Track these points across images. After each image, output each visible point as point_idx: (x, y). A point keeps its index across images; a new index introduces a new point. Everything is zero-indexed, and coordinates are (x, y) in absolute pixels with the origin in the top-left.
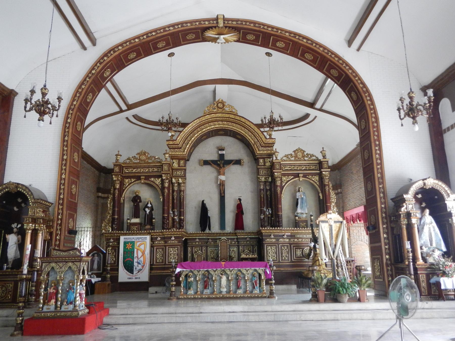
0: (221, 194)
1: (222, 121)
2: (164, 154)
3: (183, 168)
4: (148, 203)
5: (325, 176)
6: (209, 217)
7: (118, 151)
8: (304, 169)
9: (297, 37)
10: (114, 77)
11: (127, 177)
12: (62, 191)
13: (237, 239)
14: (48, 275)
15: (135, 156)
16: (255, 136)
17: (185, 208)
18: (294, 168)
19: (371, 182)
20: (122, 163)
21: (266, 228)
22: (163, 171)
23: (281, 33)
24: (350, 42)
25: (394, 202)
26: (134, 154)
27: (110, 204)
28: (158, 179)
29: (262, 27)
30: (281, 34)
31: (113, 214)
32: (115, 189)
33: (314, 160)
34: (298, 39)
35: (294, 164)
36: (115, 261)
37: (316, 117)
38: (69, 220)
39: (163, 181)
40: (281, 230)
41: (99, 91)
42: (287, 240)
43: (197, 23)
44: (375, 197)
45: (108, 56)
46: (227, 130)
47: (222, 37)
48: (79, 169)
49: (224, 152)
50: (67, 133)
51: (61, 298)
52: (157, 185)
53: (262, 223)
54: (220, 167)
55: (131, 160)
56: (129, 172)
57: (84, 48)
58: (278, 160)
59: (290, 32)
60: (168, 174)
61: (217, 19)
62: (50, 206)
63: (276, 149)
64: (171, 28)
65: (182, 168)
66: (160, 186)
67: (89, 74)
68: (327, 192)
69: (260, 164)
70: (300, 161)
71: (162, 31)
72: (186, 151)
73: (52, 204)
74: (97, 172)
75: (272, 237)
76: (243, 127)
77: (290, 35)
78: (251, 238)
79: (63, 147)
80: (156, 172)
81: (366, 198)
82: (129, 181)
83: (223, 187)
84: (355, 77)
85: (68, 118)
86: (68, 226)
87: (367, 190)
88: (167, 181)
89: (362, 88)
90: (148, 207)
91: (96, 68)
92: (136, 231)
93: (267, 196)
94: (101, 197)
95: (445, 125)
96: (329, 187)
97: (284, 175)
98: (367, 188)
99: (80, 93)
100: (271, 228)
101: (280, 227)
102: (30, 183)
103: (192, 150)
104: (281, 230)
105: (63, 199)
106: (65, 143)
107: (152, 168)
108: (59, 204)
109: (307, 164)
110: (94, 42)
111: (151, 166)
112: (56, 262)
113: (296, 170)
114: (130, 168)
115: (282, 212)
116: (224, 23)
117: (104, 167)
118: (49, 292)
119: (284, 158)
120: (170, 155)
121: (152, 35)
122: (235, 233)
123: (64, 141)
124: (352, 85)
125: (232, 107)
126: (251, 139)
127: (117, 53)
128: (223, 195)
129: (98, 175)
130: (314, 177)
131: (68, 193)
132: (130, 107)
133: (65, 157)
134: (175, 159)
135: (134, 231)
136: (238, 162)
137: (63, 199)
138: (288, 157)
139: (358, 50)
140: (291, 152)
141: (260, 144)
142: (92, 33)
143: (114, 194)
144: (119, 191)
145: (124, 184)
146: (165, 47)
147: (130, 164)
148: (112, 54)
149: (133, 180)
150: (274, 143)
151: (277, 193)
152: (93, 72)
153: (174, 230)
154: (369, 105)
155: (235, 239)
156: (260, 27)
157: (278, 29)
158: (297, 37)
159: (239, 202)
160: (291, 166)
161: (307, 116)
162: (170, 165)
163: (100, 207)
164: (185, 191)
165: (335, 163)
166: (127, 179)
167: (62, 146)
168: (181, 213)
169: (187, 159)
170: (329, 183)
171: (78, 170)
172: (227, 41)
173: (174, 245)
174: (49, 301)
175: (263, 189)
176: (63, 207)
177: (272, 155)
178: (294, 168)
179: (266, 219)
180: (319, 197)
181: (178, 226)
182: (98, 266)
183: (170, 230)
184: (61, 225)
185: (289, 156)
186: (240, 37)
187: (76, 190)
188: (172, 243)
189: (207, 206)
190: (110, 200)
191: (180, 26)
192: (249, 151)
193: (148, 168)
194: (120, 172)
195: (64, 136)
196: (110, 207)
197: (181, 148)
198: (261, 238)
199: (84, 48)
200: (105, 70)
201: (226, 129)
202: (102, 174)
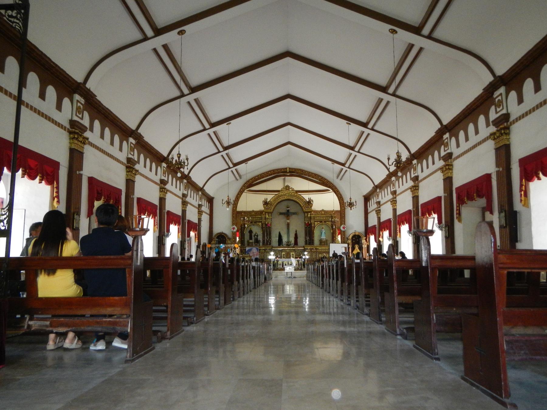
24: (338, 177)
34: (317, 177)
39: (262, 224)
42: (315, 250)
49: (289, 209)
57: (237, 180)
59: (314, 174)
61: (286, 168)
64: (270, 172)
78: (301, 249)
85: (234, 208)
90: (256, 235)
95: (369, 211)
97: (316, 221)
99: (237, 199)
102: (222, 231)
116: (289, 170)
123: (233, 216)
125: (293, 189)
127: (250, 183)
139: (341, 179)
152: (242, 190)
156: (302, 172)
157: (309, 172)
168: (270, 238)
175: (307, 227)
181: (268, 243)
195: (233, 215)
199: (237, 180)
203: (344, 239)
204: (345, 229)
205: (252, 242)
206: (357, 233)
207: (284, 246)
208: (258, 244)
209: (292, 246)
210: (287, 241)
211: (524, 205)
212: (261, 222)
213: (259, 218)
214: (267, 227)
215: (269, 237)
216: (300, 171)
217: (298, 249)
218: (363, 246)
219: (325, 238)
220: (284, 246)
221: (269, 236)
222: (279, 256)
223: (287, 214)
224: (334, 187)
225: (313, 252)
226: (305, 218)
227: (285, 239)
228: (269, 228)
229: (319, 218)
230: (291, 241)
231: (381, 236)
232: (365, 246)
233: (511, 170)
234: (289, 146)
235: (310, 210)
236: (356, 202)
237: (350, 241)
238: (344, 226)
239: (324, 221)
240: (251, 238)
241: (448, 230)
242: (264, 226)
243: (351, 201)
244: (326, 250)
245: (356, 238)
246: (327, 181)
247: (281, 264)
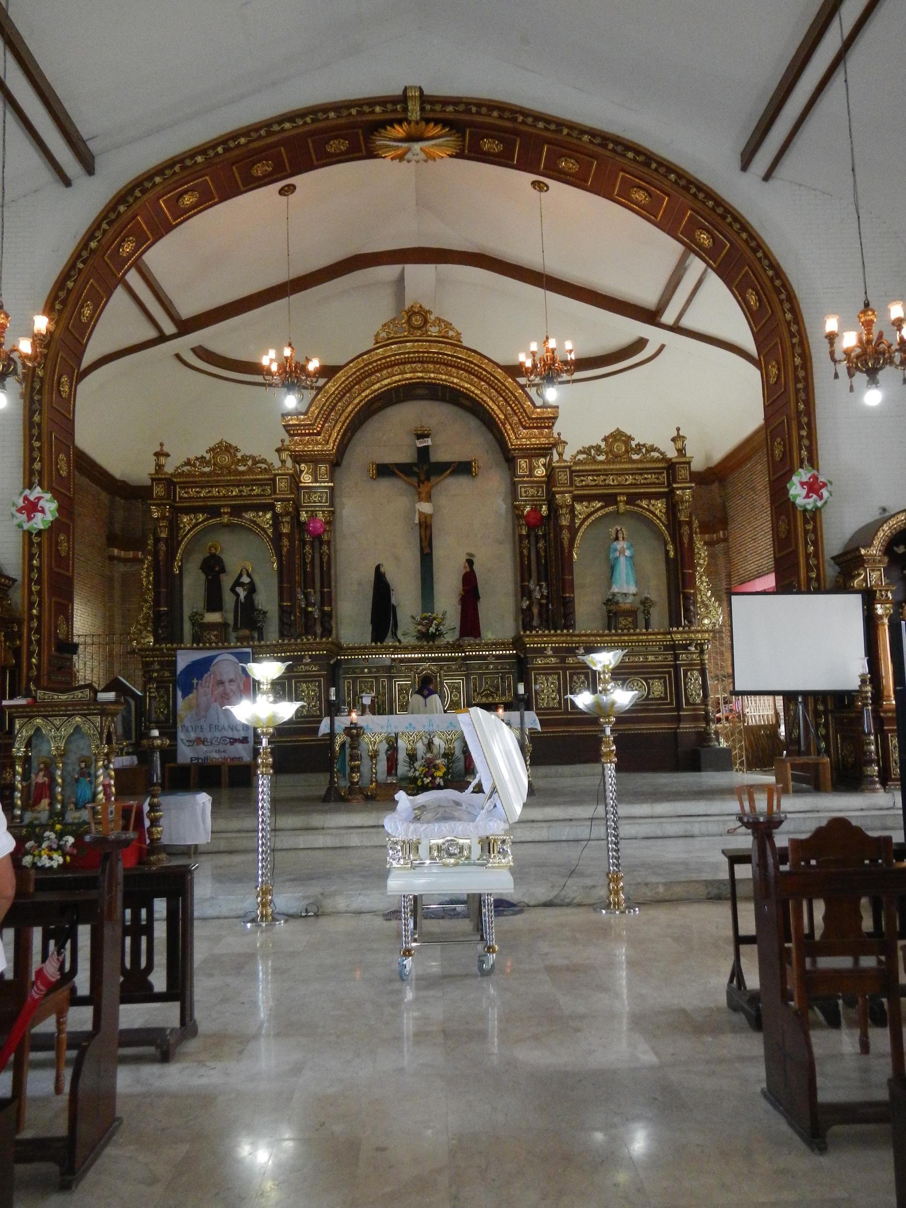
0: (422, 549)
1: (422, 362)
2: (278, 450)
3: (326, 484)
4: (240, 576)
5: (682, 502)
6: (394, 608)
7: (162, 445)
8: (631, 484)
9: (611, 146)
10: (144, 257)
11: (188, 511)
12: (35, 550)
14: (29, 744)
15: (205, 455)
16: (505, 400)
17: (333, 584)
18: (605, 480)
19: (788, 517)
20: (171, 475)
21: (534, 632)
22: (274, 492)
23: (568, 134)
24: (746, 160)
25: (838, 564)
26: (202, 452)
27: (148, 576)
28: (264, 515)
29: (520, 119)
30: (569, 139)
31: (157, 602)
32: (157, 540)
33: (657, 460)
34: (613, 150)
35: (605, 470)
36: (167, 716)
37: (662, 347)
38: (57, 617)
40: (572, 635)
41: (109, 295)
43: (354, 111)
44: (795, 552)
45: (128, 202)
46: (435, 384)
47: (417, 147)
48: (72, 496)
49: (428, 442)
50: (36, 406)
51: (63, 795)
52: (263, 529)
53: (525, 619)
54: (420, 482)
55: (194, 465)
56: (190, 498)
57: (67, 182)
58: (565, 461)
59: (593, 133)
60: (288, 500)
61: (403, 99)
62: (10, 587)
63: (559, 434)
64: (287, 125)
65: (323, 484)
66: (270, 531)
67: (82, 250)
68: (686, 540)
69: (520, 472)
70: (621, 462)
71: (263, 132)
72: (331, 441)
73: (14, 581)
74: (104, 497)
75: (550, 653)
76: (477, 376)
77: (591, 142)
78: (498, 657)
79: (31, 440)
80: (258, 495)
81: (774, 557)
82: (191, 520)
83: (428, 532)
84: (755, 251)
86: (56, 634)
87: (778, 536)
88: (288, 519)
89: (771, 280)
90: (242, 585)
91: (98, 234)
92: (217, 643)
93: (538, 552)
94: (119, 559)
96: (691, 528)
98: (777, 533)
99: (64, 302)
100: (547, 632)
101: (567, 628)
103: (347, 437)
104: (572, 635)
105: (39, 569)
106: (35, 431)
107: (247, 486)
108: (30, 580)
109: (638, 469)
110: (88, 163)
111: (246, 480)
112: (45, 717)
113: (609, 485)
114: (192, 487)
115: (573, 593)
116: (422, 109)
117: (124, 482)
118: (33, 783)
119: (581, 457)
120: (291, 451)
121: (239, 145)
122: (460, 646)
124: (747, 272)
125: (448, 325)
126: (496, 408)
128: (427, 551)
129: (107, 502)
130: (653, 502)
131: (50, 557)
132: (186, 327)
133: (37, 466)
134: (306, 462)
135: (210, 644)
136: (464, 468)
137: (39, 569)
138: (589, 454)
139: (767, 177)
140: (596, 439)
141: (520, 420)
142: (84, 142)
143: (156, 554)
144: (167, 546)
145: (179, 529)
146: (270, 174)
147: (194, 476)
148: (137, 198)
149: (201, 517)
150: (555, 418)
151: (562, 543)
152: (93, 245)
153: (308, 640)
154: (788, 323)
155: (459, 660)
156: (514, 120)
157: (560, 124)
158: (611, 146)
159: (468, 569)
160: (598, 476)
161: (641, 343)
162: (295, 478)
163: (117, 585)
164: (333, 543)
165: (712, 465)
166: (187, 514)
167: (27, 439)
169: (335, 461)
170: (690, 517)
171: (70, 498)
172: (430, 157)
173: (311, 676)
174: (37, 801)
176: (41, 589)
177: (550, 449)
178: (605, 480)
179: (535, 611)
180: (667, 552)
181: (319, 631)
182: (124, 728)
183: (299, 640)
184: (38, 631)
185: (593, 452)
186: (464, 146)
187: (69, 546)
188: (306, 671)
189: (389, 577)
190: (147, 568)
191: (308, 120)
192: (490, 436)
193: (238, 486)
194: (169, 498)
196: (148, 584)
197: (319, 434)
198: (522, 656)
199: (67, 182)
200: (123, 240)
201: (428, 383)
202: (117, 499)
203: (817, 567)
204: (825, 492)
205: (224, 625)
207: (405, 641)
208: (256, 635)
209: (450, 638)
210: (418, 618)
212: (271, 507)
214: (308, 538)
215: (322, 593)
216: (495, 114)
217: (485, 658)
219: (633, 589)
220: (405, 641)
221: (322, 587)
222: (367, 701)
224: (729, 220)
226: (514, 485)
228: (321, 543)
230: (444, 614)
235: (544, 441)
237: (874, 577)
238: (815, 478)
239: (627, 494)
240: (214, 602)
242: (285, 530)
244: (651, 658)
246: (683, 182)
247: (383, 757)
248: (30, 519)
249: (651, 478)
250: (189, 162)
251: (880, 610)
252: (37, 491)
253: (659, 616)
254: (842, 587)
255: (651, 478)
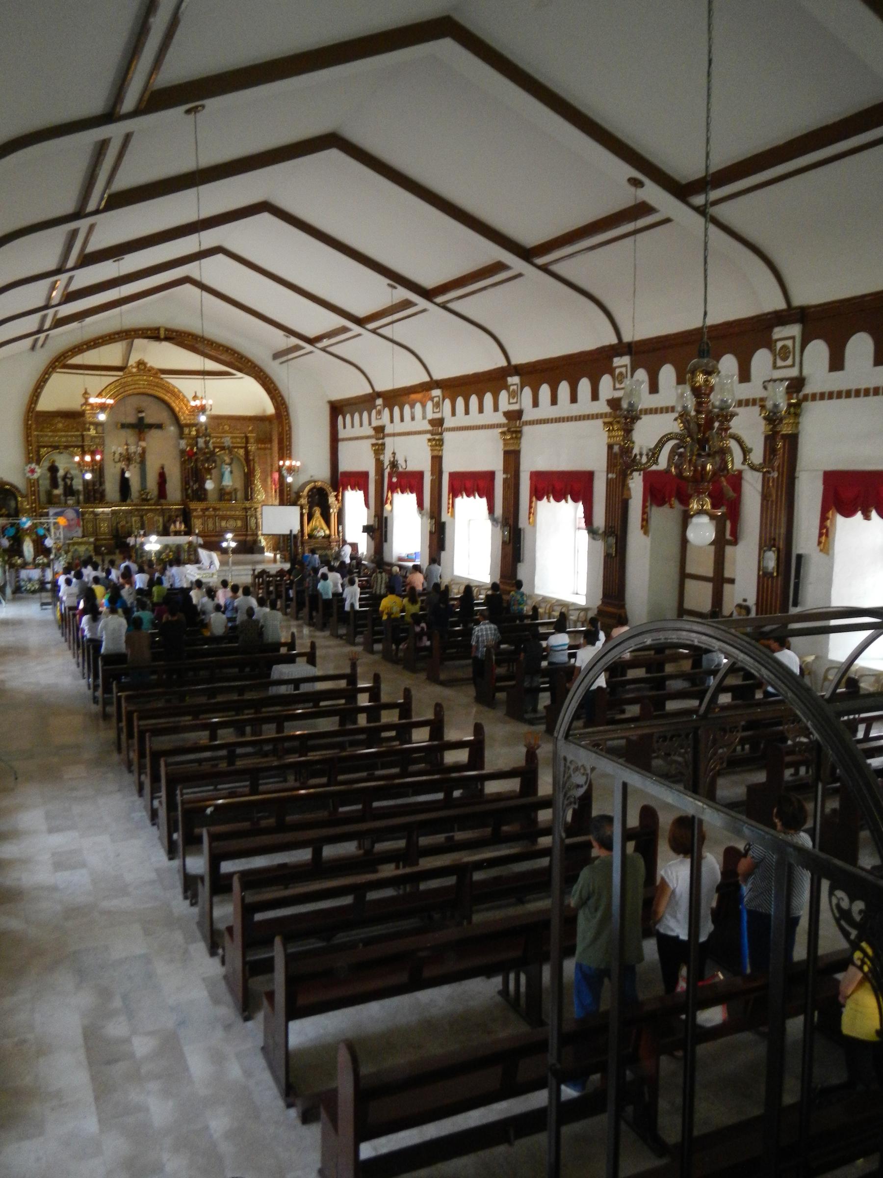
5: (250, 451)
11: (44, 447)
13: (162, 509)
49: (143, 415)
61: (158, 329)
90: (68, 478)
136: (159, 426)
139: (282, 363)
149: (50, 449)
203: (289, 495)
206: (319, 484)
211: (821, 550)
213: (76, 436)
218: (331, 510)
223: (140, 427)
225: (209, 517)
227: (135, 485)
229: (218, 440)
231: (389, 502)
232: (333, 511)
233: (796, 481)
234: (188, 287)
236: (406, 461)
237: (304, 501)
241: (616, 543)
243: (394, 457)
245: (312, 493)
248: (33, 475)
249: (238, 440)
250: (81, 348)
251: (304, 511)
252: (33, 466)
253: (240, 495)
254: (294, 504)
255: (238, 440)
